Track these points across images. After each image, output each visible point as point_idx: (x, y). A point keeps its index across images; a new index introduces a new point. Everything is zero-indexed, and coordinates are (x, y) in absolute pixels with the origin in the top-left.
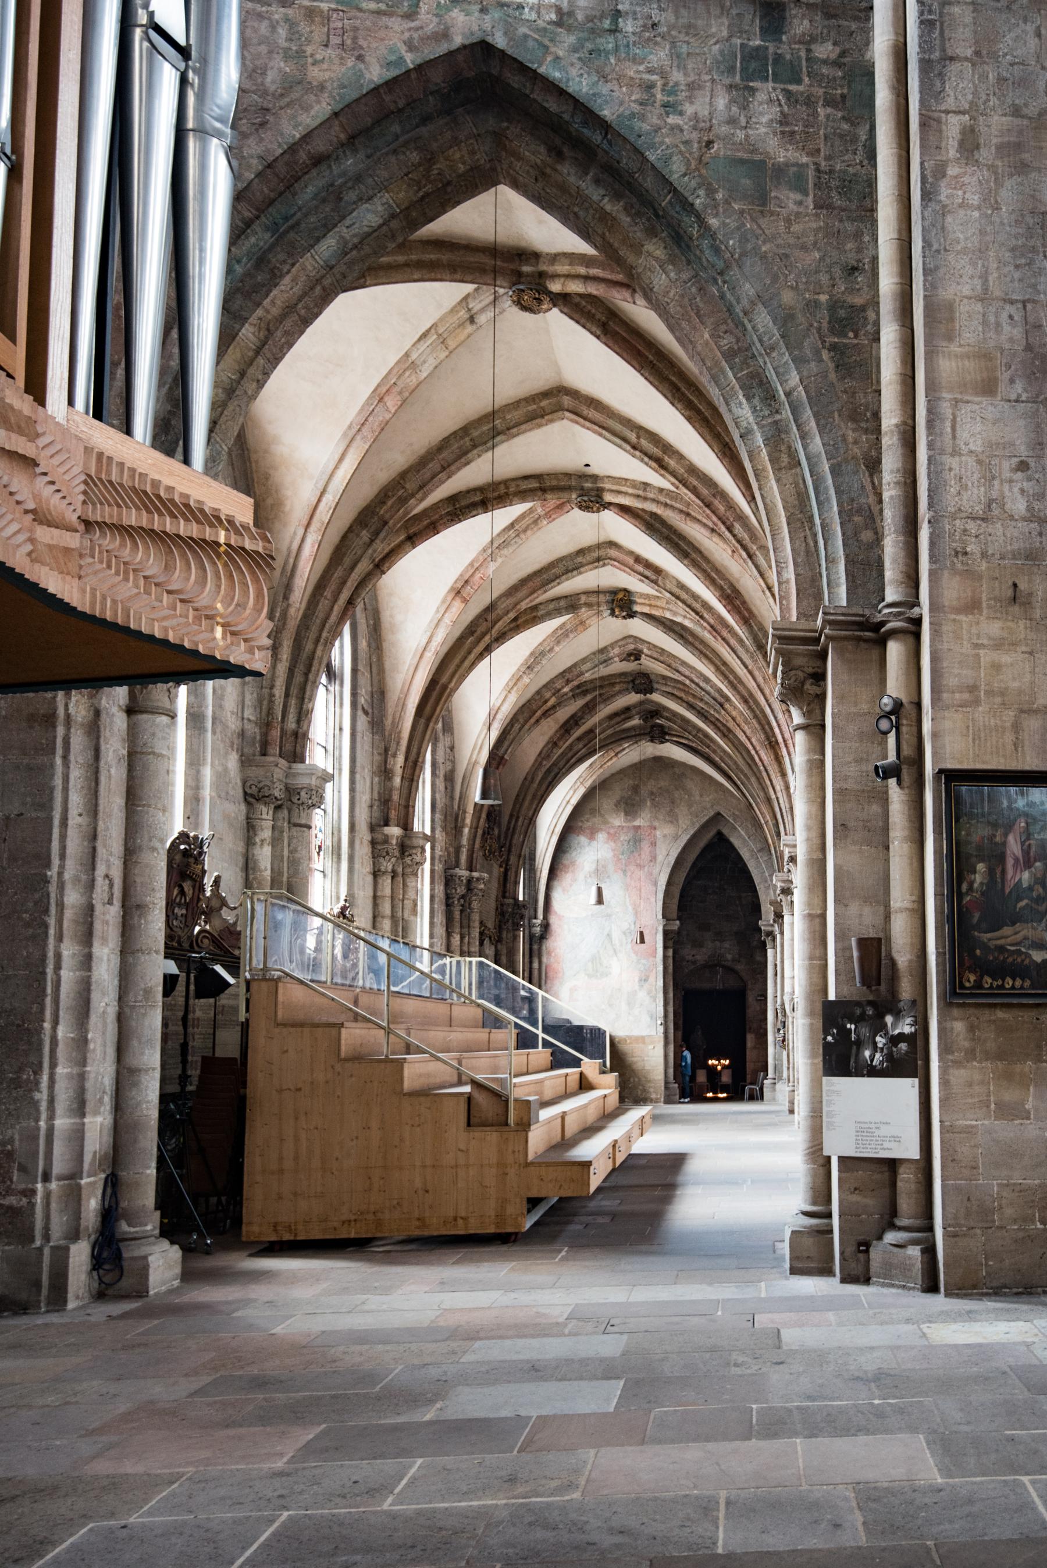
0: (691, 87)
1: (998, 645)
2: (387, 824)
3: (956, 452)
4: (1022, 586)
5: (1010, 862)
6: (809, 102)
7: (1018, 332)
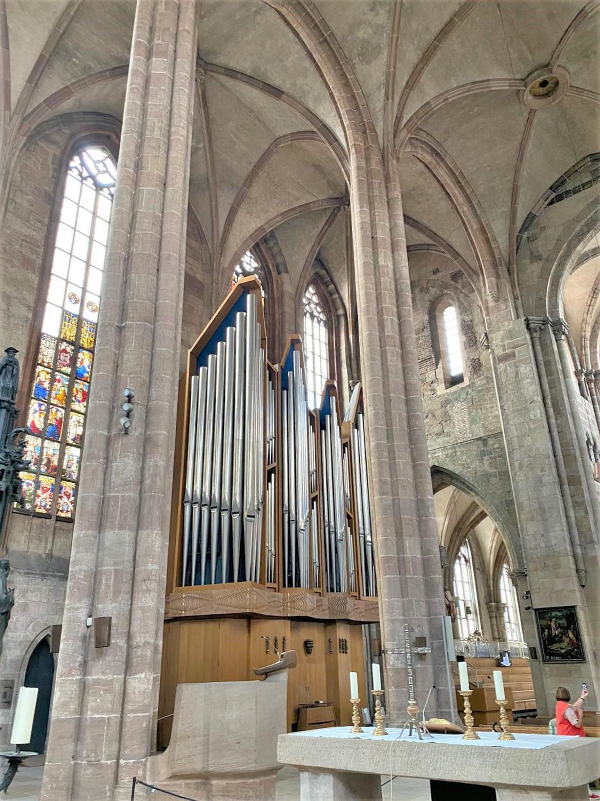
0: (471, 462)
1: (544, 578)
2: (491, 602)
3: (528, 535)
4: (547, 563)
5: (553, 629)
6: (495, 458)
7: (537, 506)
